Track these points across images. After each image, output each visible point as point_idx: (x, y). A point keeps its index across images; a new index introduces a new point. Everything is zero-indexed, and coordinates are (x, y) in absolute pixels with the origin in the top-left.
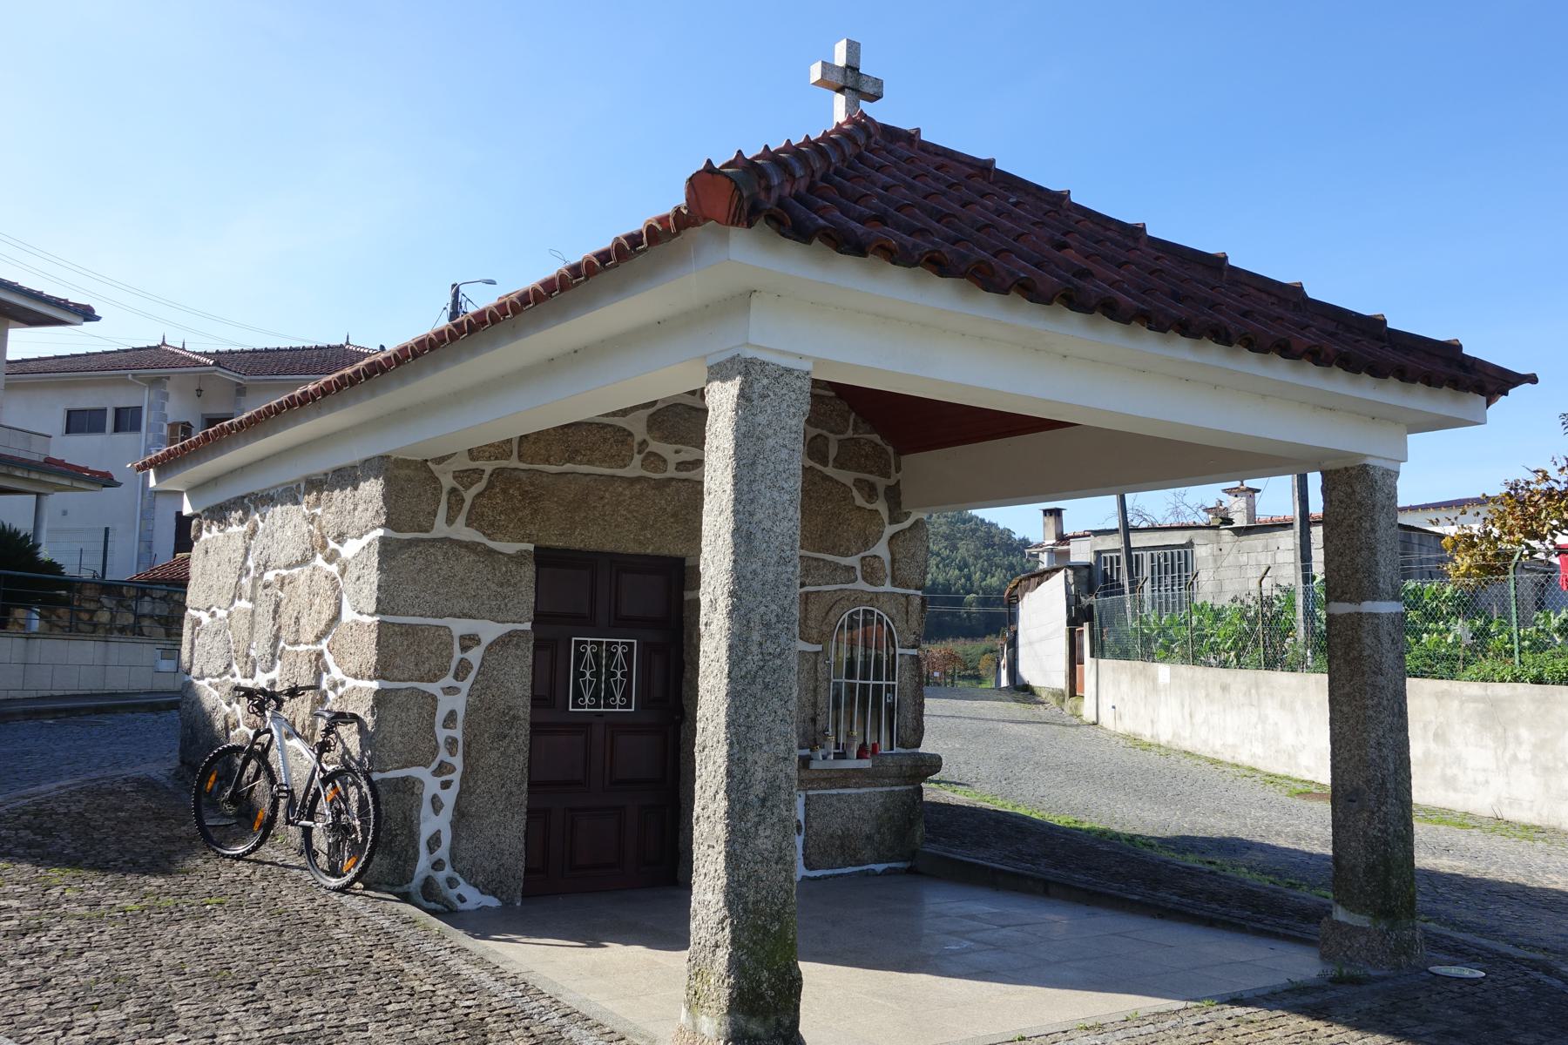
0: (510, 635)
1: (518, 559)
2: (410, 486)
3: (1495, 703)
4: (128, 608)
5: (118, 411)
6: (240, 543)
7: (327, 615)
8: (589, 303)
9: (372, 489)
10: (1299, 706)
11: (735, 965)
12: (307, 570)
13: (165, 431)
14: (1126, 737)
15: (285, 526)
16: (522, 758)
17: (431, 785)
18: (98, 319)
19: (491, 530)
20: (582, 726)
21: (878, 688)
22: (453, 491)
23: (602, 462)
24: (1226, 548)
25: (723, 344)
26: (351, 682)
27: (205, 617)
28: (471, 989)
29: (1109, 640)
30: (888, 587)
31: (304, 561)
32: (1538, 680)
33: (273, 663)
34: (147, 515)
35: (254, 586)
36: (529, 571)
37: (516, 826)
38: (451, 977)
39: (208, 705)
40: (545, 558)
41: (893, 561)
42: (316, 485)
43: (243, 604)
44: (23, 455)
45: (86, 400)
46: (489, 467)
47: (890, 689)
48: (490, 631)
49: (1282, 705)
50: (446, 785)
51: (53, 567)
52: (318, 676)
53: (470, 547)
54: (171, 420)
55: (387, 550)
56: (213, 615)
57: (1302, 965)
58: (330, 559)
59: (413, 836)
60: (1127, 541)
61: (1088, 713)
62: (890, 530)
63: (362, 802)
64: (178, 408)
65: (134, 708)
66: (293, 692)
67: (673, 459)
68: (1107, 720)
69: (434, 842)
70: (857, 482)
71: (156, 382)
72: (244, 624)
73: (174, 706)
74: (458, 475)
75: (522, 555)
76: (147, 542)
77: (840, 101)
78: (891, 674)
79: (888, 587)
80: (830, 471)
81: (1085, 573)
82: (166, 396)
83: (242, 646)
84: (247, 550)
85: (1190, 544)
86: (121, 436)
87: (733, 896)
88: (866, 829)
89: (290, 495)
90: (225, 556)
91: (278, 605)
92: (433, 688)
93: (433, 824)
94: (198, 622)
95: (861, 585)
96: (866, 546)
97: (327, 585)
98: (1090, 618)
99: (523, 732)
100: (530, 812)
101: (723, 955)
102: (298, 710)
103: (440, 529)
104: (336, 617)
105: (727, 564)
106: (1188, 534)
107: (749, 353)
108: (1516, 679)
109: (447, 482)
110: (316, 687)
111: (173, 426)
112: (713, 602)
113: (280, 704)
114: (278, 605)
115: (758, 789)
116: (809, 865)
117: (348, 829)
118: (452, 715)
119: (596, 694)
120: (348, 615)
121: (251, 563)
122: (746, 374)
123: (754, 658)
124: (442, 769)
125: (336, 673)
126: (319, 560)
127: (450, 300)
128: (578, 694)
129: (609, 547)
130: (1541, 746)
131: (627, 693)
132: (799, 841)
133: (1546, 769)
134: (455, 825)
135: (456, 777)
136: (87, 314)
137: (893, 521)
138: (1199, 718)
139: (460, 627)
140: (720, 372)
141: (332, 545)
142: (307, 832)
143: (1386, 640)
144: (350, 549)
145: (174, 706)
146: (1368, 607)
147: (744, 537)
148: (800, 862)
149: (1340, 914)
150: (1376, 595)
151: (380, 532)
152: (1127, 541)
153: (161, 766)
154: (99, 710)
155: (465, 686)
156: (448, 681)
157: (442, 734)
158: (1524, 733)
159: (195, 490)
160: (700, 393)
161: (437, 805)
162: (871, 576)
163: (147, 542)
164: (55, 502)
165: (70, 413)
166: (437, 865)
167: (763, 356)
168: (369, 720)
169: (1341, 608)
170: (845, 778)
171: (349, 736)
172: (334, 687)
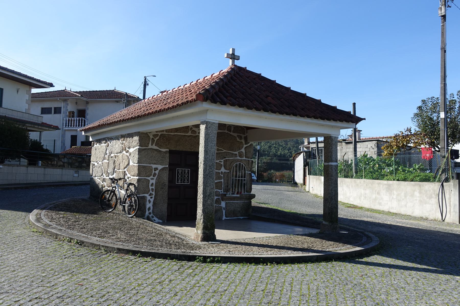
0: (164, 168)
1: (166, 152)
2: (144, 138)
3: (389, 185)
4: (61, 161)
5: (55, 108)
6: (105, 148)
7: (126, 164)
8: (180, 110)
9: (136, 138)
10: (350, 186)
11: (204, 222)
12: (121, 154)
13: (68, 114)
14: (314, 195)
15: (116, 145)
16: (167, 193)
17: (149, 198)
18: (54, 86)
19: (160, 146)
21: (242, 180)
22: (153, 139)
23: (183, 132)
24: (344, 147)
25: (203, 118)
26: (132, 177)
27: (96, 164)
28: (159, 230)
29: (312, 171)
30: (244, 158)
31: (121, 152)
32: (398, 180)
33: (114, 173)
34: (63, 136)
35: (109, 157)
36: (168, 155)
37: (166, 206)
38: (154, 229)
39: (97, 183)
40: (171, 152)
41: (246, 153)
42: (123, 136)
43: (106, 161)
44: (36, 122)
45: (47, 105)
46: (160, 134)
47: (245, 180)
48: (160, 167)
49: (347, 186)
50: (151, 198)
51: (47, 150)
52: (125, 176)
53: (156, 150)
54: (69, 111)
55: (140, 151)
56: (98, 163)
57: (315, 231)
58: (127, 152)
59: (145, 208)
60: (318, 145)
61: (307, 190)
62: (245, 146)
63: (135, 201)
64: (71, 107)
65: (71, 185)
66: (120, 179)
68: (311, 191)
69: (149, 209)
70: (238, 136)
71: (65, 101)
72: (106, 165)
73: (89, 184)
74: (153, 135)
75: (166, 151)
76: (63, 143)
77: (231, 61)
78: (245, 177)
79: (244, 158)
80: (232, 133)
81: (308, 153)
82: (68, 104)
83: (106, 170)
84: (107, 149)
86: (56, 115)
87: (204, 211)
88: (239, 209)
89: (117, 138)
90: (101, 150)
91: (114, 161)
92: (149, 178)
94: (94, 165)
95: (238, 158)
96: (240, 149)
97: (127, 157)
98: (308, 165)
99: (166, 188)
101: (202, 220)
102: (121, 183)
103: (150, 146)
104: (128, 164)
105: (203, 156)
107: (207, 120)
108: (394, 180)
109: (151, 137)
110: (124, 178)
111: (70, 112)
112: (201, 163)
113: (118, 181)
114: (114, 161)
115: (208, 194)
116: (226, 217)
117: (132, 206)
118: (152, 184)
119: (181, 180)
120: (131, 163)
121: (107, 152)
123: (208, 172)
124: (151, 194)
125: (129, 175)
126: (124, 152)
127: (144, 81)
128: (178, 180)
129: (184, 150)
130: (398, 195)
131: (188, 180)
132: (224, 211)
133: (399, 201)
134: (153, 206)
135: (153, 196)
136: (51, 85)
137: (246, 144)
139: (154, 166)
140: (203, 123)
141: (127, 149)
142: (124, 206)
143: (334, 170)
144: (131, 150)
145: (89, 184)
146: (330, 163)
147: (206, 152)
148: (224, 216)
149: (324, 222)
150: (332, 161)
151: (138, 147)
152: (318, 145)
153: (87, 196)
154: (63, 185)
155: (155, 178)
156: (152, 177)
157: (151, 188)
158: (395, 192)
159: (92, 136)
160: (199, 125)
162: (240, 156)
163: (63, 143)
164: (44, 133)
165: (42, 108)
166: (150, 213)
167: (209, 121)
168: (136, 185)
169: (326, 164)
170: (234, 198)
172: (128, 178)
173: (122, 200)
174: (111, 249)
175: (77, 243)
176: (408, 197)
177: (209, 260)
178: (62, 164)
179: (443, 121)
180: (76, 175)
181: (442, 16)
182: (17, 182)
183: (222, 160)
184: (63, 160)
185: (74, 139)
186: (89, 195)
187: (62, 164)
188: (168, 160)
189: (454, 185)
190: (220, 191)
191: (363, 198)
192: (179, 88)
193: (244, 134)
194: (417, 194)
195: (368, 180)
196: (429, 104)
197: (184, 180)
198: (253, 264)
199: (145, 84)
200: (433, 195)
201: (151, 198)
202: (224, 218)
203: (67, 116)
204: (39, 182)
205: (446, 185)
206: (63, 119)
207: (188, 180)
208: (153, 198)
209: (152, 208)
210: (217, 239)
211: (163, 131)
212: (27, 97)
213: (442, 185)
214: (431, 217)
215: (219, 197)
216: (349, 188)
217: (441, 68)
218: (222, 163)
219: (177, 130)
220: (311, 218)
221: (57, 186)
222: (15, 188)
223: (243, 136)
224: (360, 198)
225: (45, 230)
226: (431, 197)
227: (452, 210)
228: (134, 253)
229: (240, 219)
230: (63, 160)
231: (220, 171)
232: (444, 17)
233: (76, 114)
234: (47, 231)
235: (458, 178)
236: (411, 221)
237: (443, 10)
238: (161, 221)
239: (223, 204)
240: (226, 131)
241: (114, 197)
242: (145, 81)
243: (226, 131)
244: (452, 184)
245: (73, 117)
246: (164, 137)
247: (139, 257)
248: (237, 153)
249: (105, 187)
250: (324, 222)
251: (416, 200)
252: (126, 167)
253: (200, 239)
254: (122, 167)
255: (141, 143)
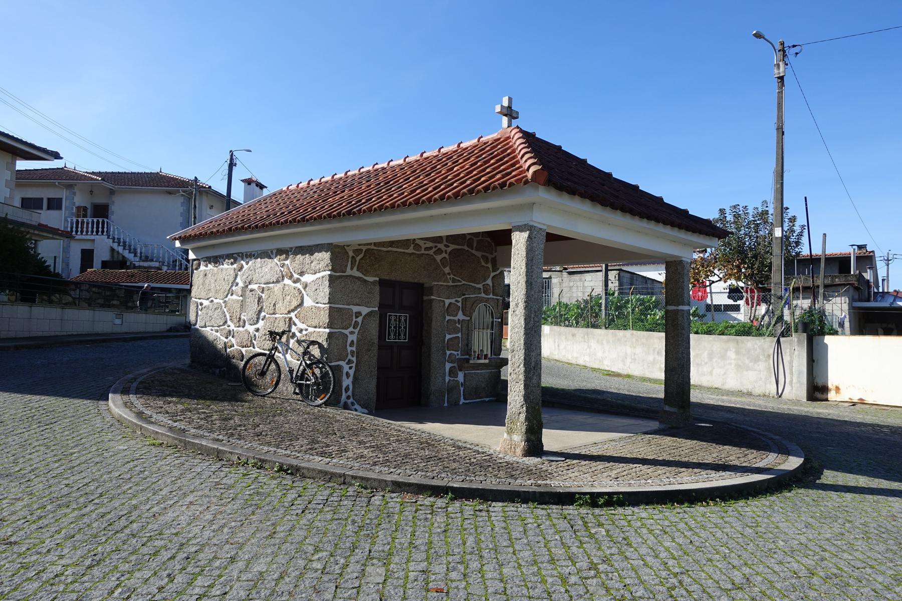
0: (371, 312)
1: (374, 283)
5: (49, 199)
6: (232, 272)
7: (295, 303)
10: (605, 342)
11: (527, 419)
12: (280, 285)
13: (74, 210)
16: (375, 358)
17: (346, 368)
18: (62, 158)
20: (390, 346)
22: (353, 257)
24: (565, 280)
26: (311, 330)
27: (206, 303)
30: (491, 296)
31: (278, 282)
33: (257, 321)
34: (66, 250)
36: (377, 288)
37: (374, 382)
39: (211, 338)
40: (383, 283)
41: (493, 286)
42: (280, 252)
44: (28, 222)
45: (32, 193)
46: (364, 248)
48: (365, 310)
49: (598, 341)
50: (351, 368)
52: (290, 326)
53: (359, 278)
54: (77, 205)
56: (212, 301)
62: (492, 274)
64: (80, 200)
65: (117, 340)
67: (423, 246)
69: (347, 389)
70: (483, 256)
71: (69, 187)
74: (354, 251)
76: (66, 264)
80: (474, 252)
82: (74, 194)
84: (236, 275)
85: (550, 278)
86: (49, 212)
88: (483, 385)
89: (266, 255)
90: (220, 276)
92: (346, 332)
93: (347, 382)
94: (201, 304)
96: (485, 280)
97: (296, 292)
99: (375, 349)
100: (378, 378)
101: (523, 417)
103: (349, 272)
104: (301, 304)
106: (550, 273)
107: (531, 223)
109: (351, 254)
110: (290, 331)
111: (78, 208)
112: (517, 305)
116: (465, 399)
118: (352, 341)
119: (395, 335)
120: (308, 302)
121: (238, 280)
122: (530, 230)
124: (350, 362)
127: (229, 157)
128: (389, 335)
131: (405, 335)
132: (462, 389)
134: (353, 383)
135: (354, 365)
136: (56, 156)
137: (494, 271)
138: (562, 347)
139: (355, 309)
140: (521, 229)
146: (681, 307)
149: (667, 408)
151: (329, 273)
154: (104, 341)
155: (357, 331)
156: (351, 329)
157: (349, 349)
159: (194, 250)
161: (348, 374)
162: (486, 292)
165: (23, 199)
166: (348, 397)
167: (535, 225)
169: (671, 308)
171: (316, 351)
173: (295, 373)
174: (376, 484)
175: (281, 469)
176: (714, 360)
177: (602, 501)
178: (70, 299)
179: (779, 241)
180: (118, 321)
181: (779, 78)
182: (12, 335)
183: (460, 299)
184: (72, 293)
185: (87, 256)
186: (188, 361)
187: (70, 299)
188: (377, 298)
189: (799, 341)
190: (455, 353)
191: (629, 360)
192: (376, 167)
193: (492, 254)
194: (732, 354)
195: (639, 332)
196: (729, 218)
197: (399, 335)
198: (686, 505)
199: (232, 165)
200: (761, 357)
201: (351, 368)
202: (462, 401)
203: (72, 214)
204: (53, 334)
205: (785, 342)
206: (66, 220)
207: (405, 335)
208: (353, 369)
209: (351, 387)
210: (545, 449)
211: (370, 244)
212: (8, 175)
213: (778, 342)
214: (758, 391)
215: (455, 365)
216: (602, 344)
217: (777, 158)
218: (460, 304)
219: (392, 243)
220: (594, 396)
221: (93, 341)
222: (16, 348)
223: (490, 257)
224: (623, 361)
225: (180, 441)
226: (756, 360)
227: (795, 380)
228: (437, 491)
229: (484, 402)
230: (72, 293)
231: (456, 318)
232: (781, 78)
233: (89, 211)
234: (186, 443)
235: (804, 331)
236: (743, 399)
237: (782, 69)
238: (366, 411)
239: (461, 377)
240: (466, 248)
241: (273, 366)
242: (232, 159)
243: (466, 248)
244: (796, 340)
245: (85, 216)
246: (371, 255)
247: (452, 499)
248: (480, 286)
249: (232, 346)
250: (667, 408)
251: (730, 364)
252: (293, 311)
253: (519, 451)
254: (282, 308)
255: (337, 264)
